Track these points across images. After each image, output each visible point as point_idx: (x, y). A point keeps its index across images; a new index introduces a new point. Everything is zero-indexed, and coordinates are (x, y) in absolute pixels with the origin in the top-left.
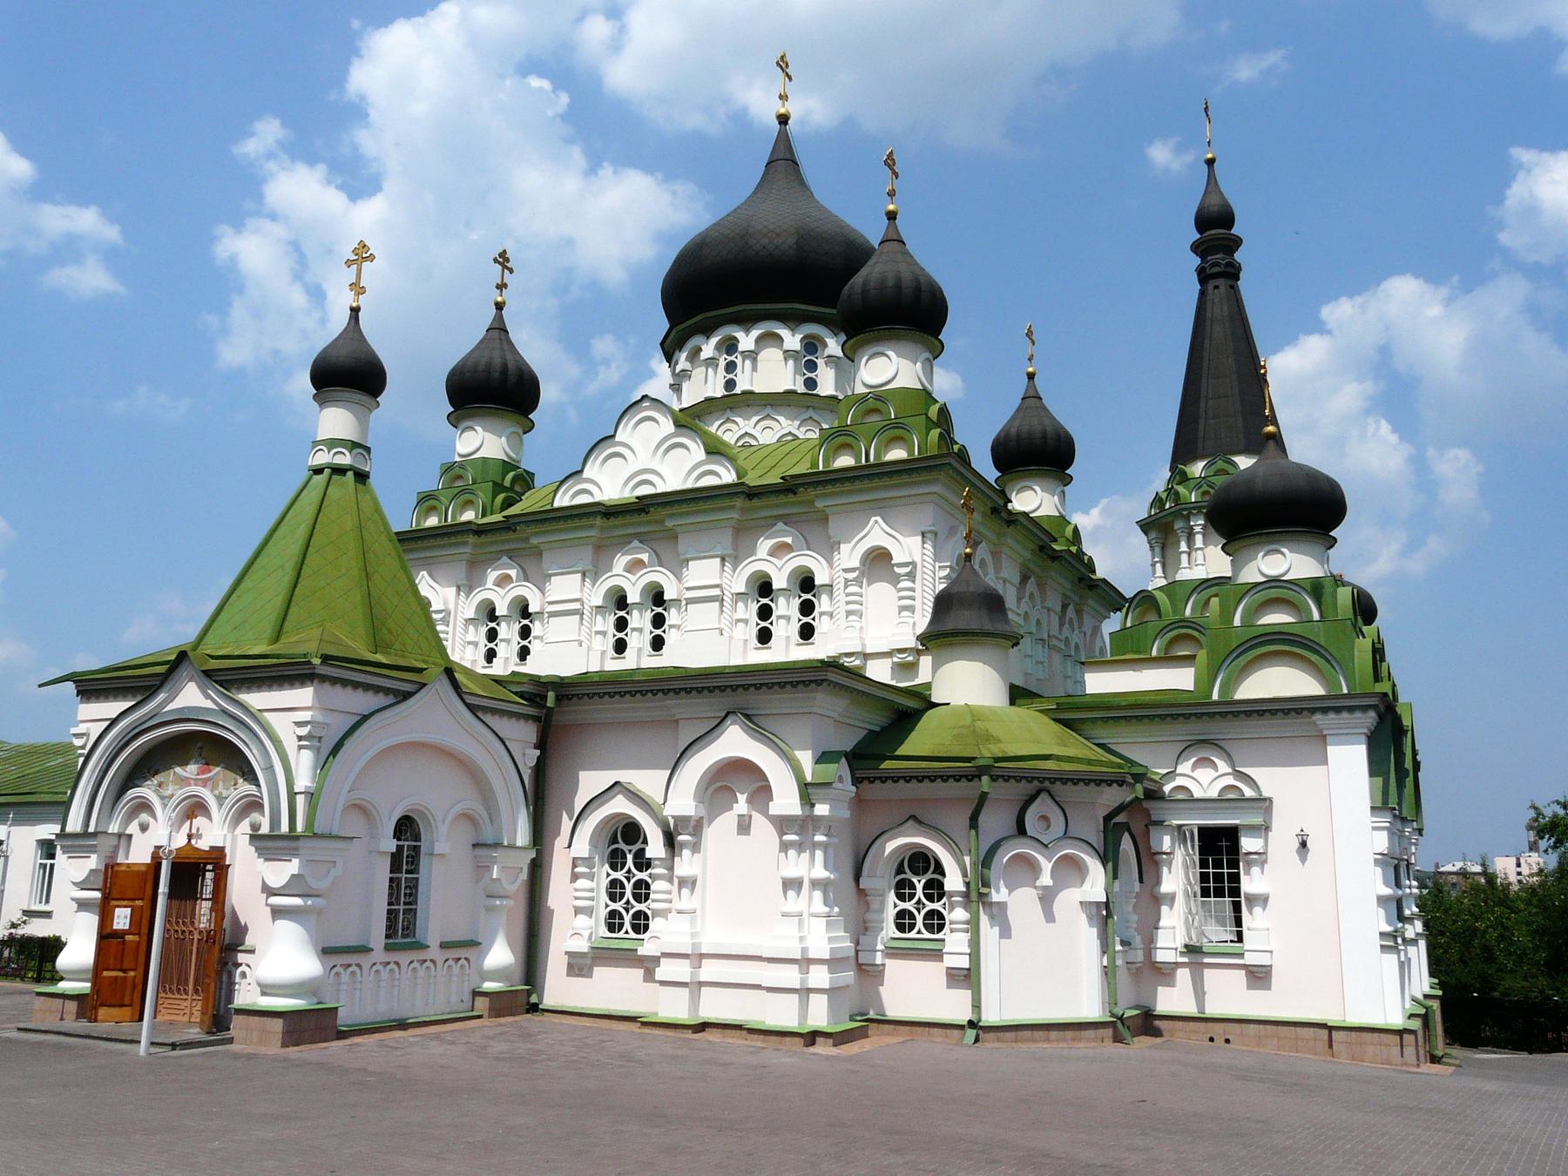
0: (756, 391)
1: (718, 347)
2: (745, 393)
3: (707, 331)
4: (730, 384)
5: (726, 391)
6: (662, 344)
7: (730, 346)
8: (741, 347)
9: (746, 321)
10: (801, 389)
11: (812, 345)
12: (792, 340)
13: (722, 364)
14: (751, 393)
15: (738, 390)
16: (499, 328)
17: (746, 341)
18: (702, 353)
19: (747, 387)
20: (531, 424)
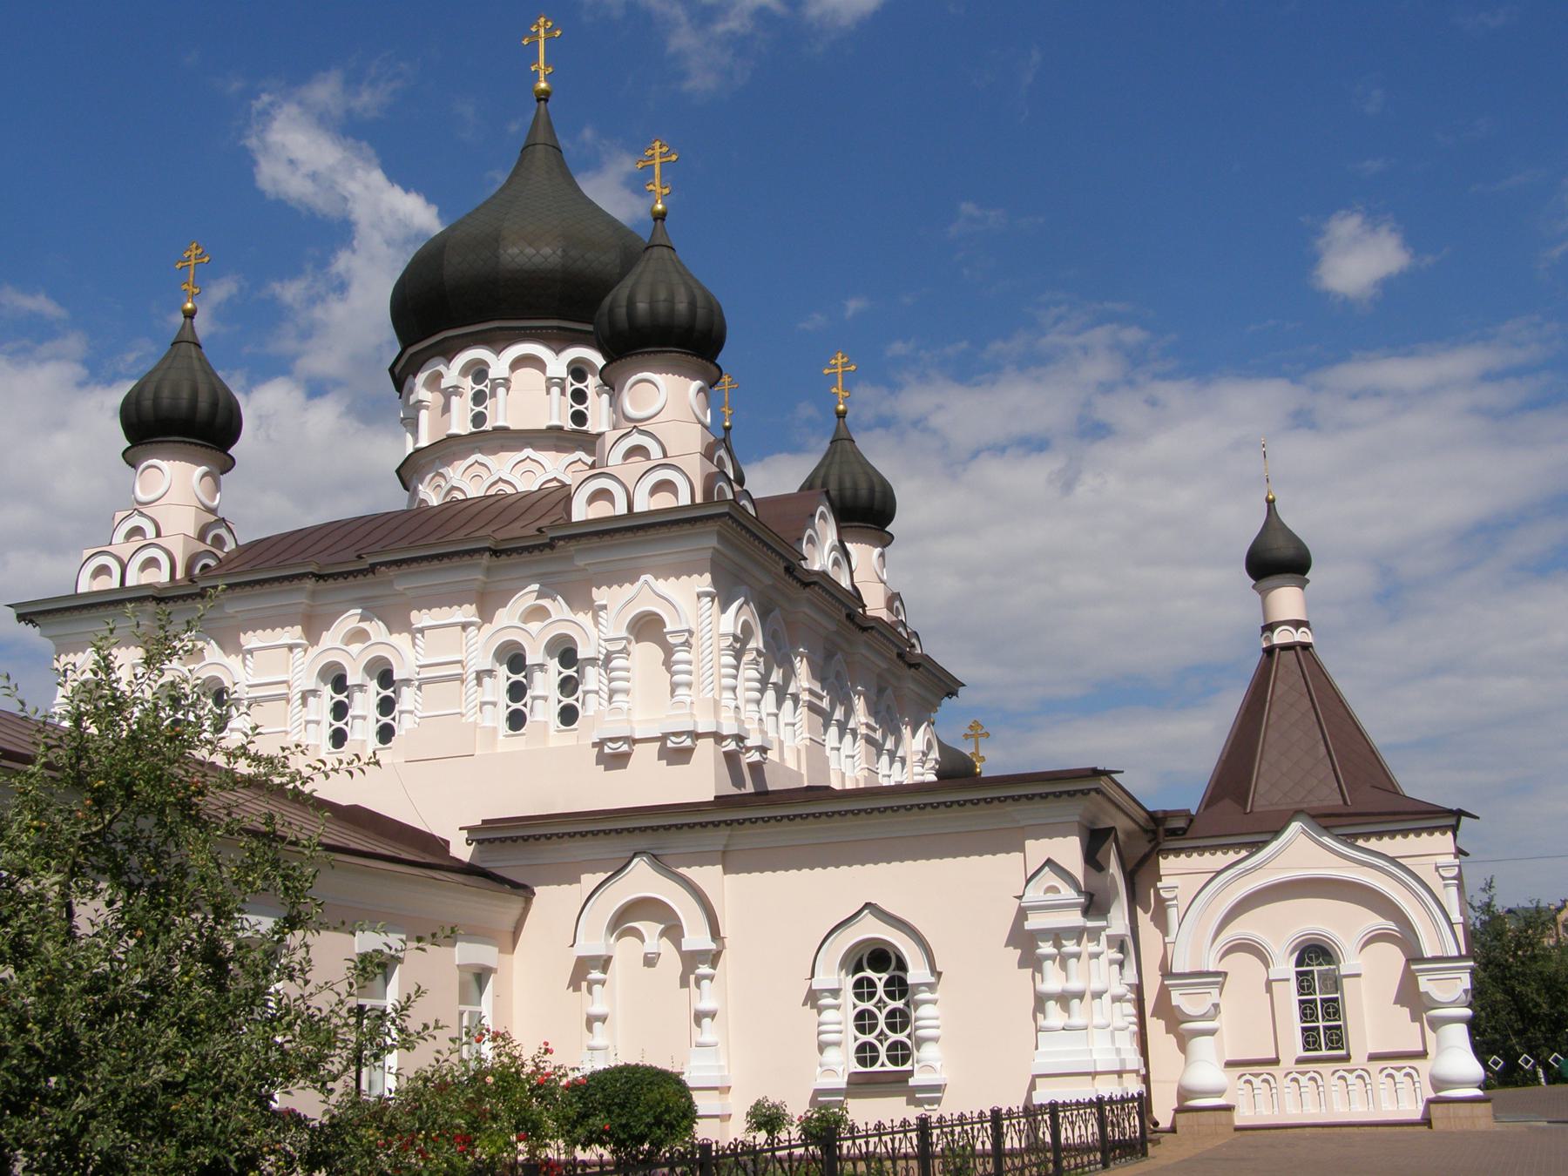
0: (512, 428)
1: (464, 372)
2: (496, 429)
3: (448, 352)
4: (479, 419)
5: (474, 427)
6: (392, 370)
7: (478, 371)
8: (492, 374)
9: (497, 341)
10: (569, 425)
11: (578, 371)
12: (557, 363)
13: (469, 394)
14: (505, 429)
15: (488, 426)
17: (499, 364)
18: (443, 380)
19: (500, 423)
20: (231, 462)
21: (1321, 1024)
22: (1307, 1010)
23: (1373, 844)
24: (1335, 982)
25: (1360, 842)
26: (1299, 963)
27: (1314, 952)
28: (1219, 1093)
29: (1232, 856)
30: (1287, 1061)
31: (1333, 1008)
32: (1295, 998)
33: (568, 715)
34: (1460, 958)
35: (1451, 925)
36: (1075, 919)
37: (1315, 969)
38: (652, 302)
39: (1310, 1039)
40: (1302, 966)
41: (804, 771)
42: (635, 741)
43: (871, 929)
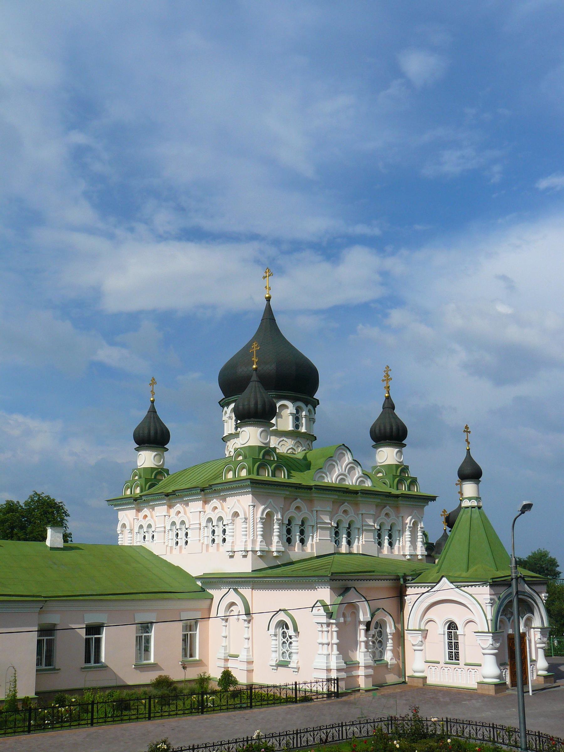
16: (153, 411)
21: (453, 651)
22: (450, 644)
23: (465, 589)
24: (456, 637)
25: (462, 588)
26: (449, 628)
27: (452, 626)
28: (423, 672)
29: (427, 589)
30: (442, 664)
31: (457, 644)
32: (447, 641)
33: (224, 540)
34: (489, 632)
35: (487, 621)
36: (324, 620)
37: (452, 631)
38: (243, 405)
39: (450, 658)
40: (450, 630)
41: (315, 551)
42: (234, 552)
43: (282, 616)
